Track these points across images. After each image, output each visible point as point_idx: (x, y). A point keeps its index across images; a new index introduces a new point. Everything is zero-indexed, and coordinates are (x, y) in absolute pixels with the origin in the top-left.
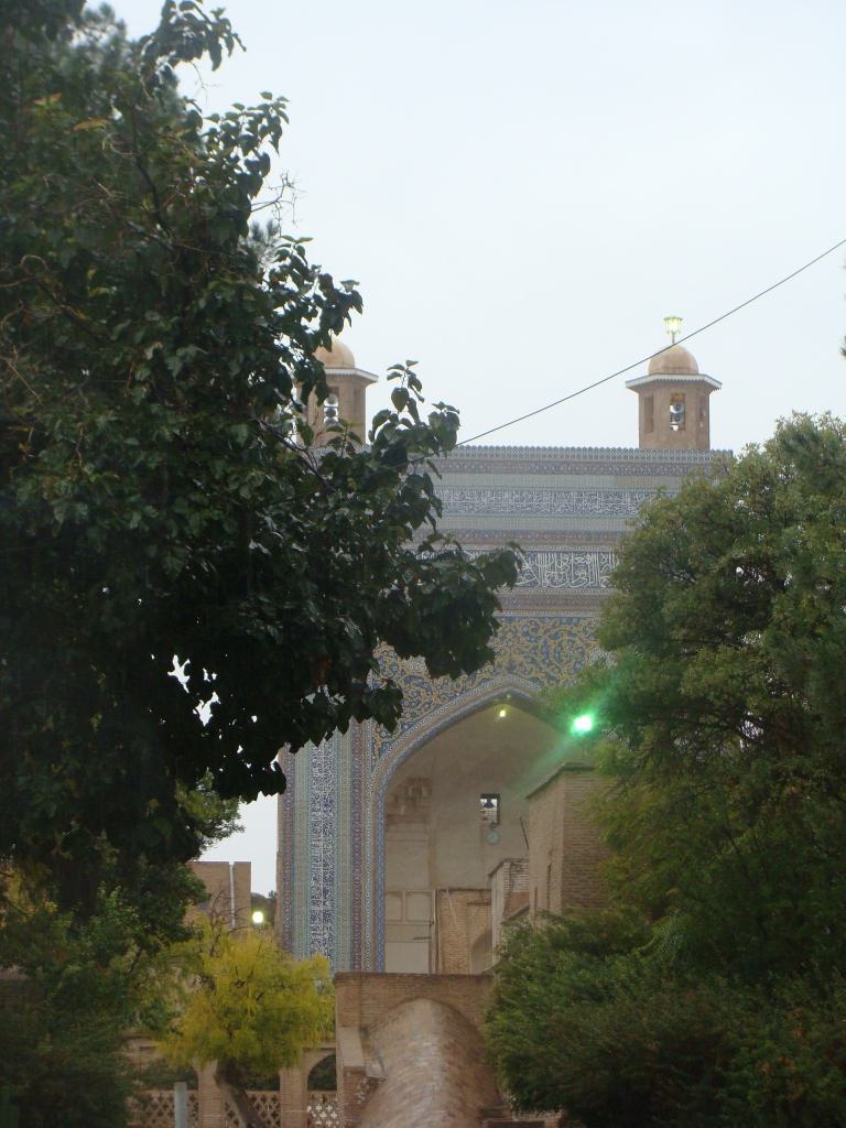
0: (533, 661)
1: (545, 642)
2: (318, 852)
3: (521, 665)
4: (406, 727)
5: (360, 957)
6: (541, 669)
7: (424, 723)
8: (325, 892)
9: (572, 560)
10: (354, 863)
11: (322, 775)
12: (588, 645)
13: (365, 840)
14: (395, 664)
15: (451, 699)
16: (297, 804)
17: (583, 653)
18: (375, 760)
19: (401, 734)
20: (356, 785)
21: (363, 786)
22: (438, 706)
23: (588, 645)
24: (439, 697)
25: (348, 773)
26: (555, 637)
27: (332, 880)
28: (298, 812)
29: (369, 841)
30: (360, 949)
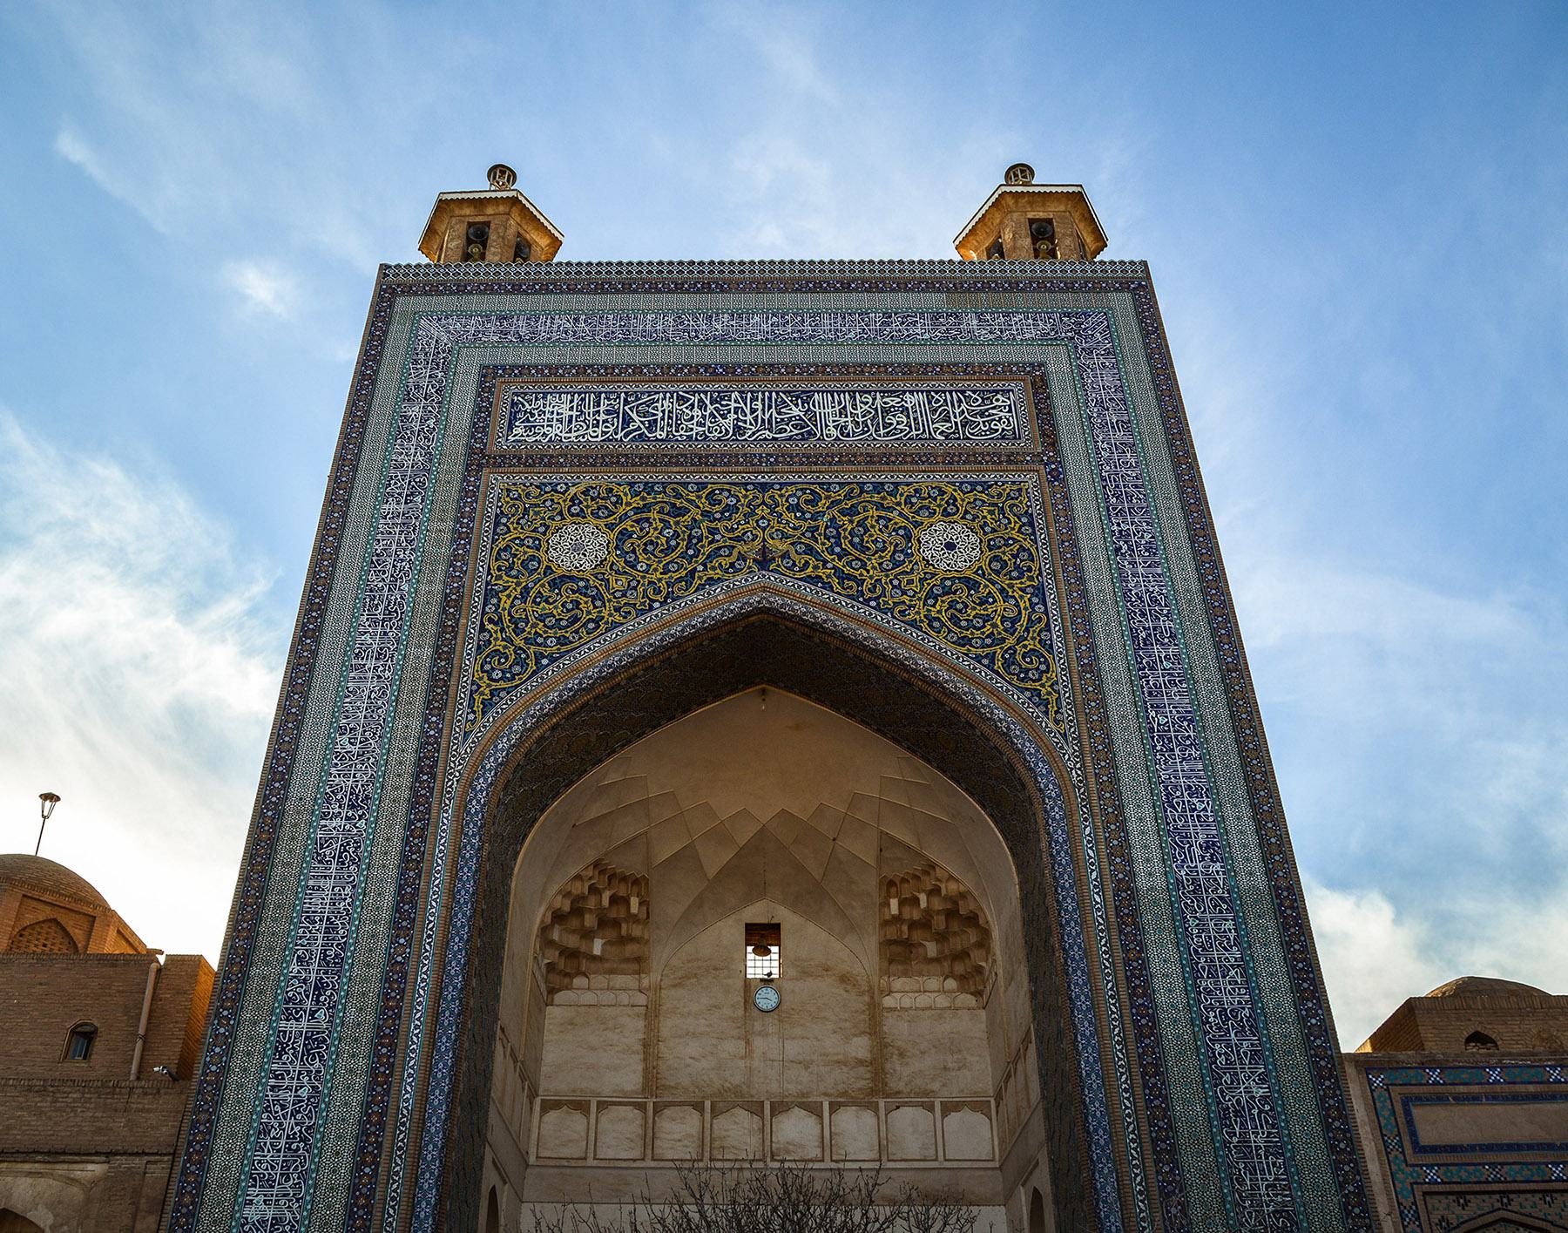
0: (809, 550)
1: (833, 519)
2: (320, 903)
3: (785, 555)
4: (545, 661)
5: (380, 1145)
6: (825, 562)
7: (583, 654)
8: (320, 987)
9: (878, 400)
10: (395, 925)
11: (355, 749)
12: (917, 524)
13: (430, 874)
14: (533, 558)
15: (643, 612)
16: (290, 806)
17: (908, 537)
18: (473, 722)
19: (534, 673)
20: (427, 767)
21: (439, 770)
22: (615, 625)
23: (917, 524)
24: (617, 610)
25: (412, 745)
26: (852, 512)
27: (339, 961)
28: (289, 820)
29: (439, 879)
30: (381, 1125)
